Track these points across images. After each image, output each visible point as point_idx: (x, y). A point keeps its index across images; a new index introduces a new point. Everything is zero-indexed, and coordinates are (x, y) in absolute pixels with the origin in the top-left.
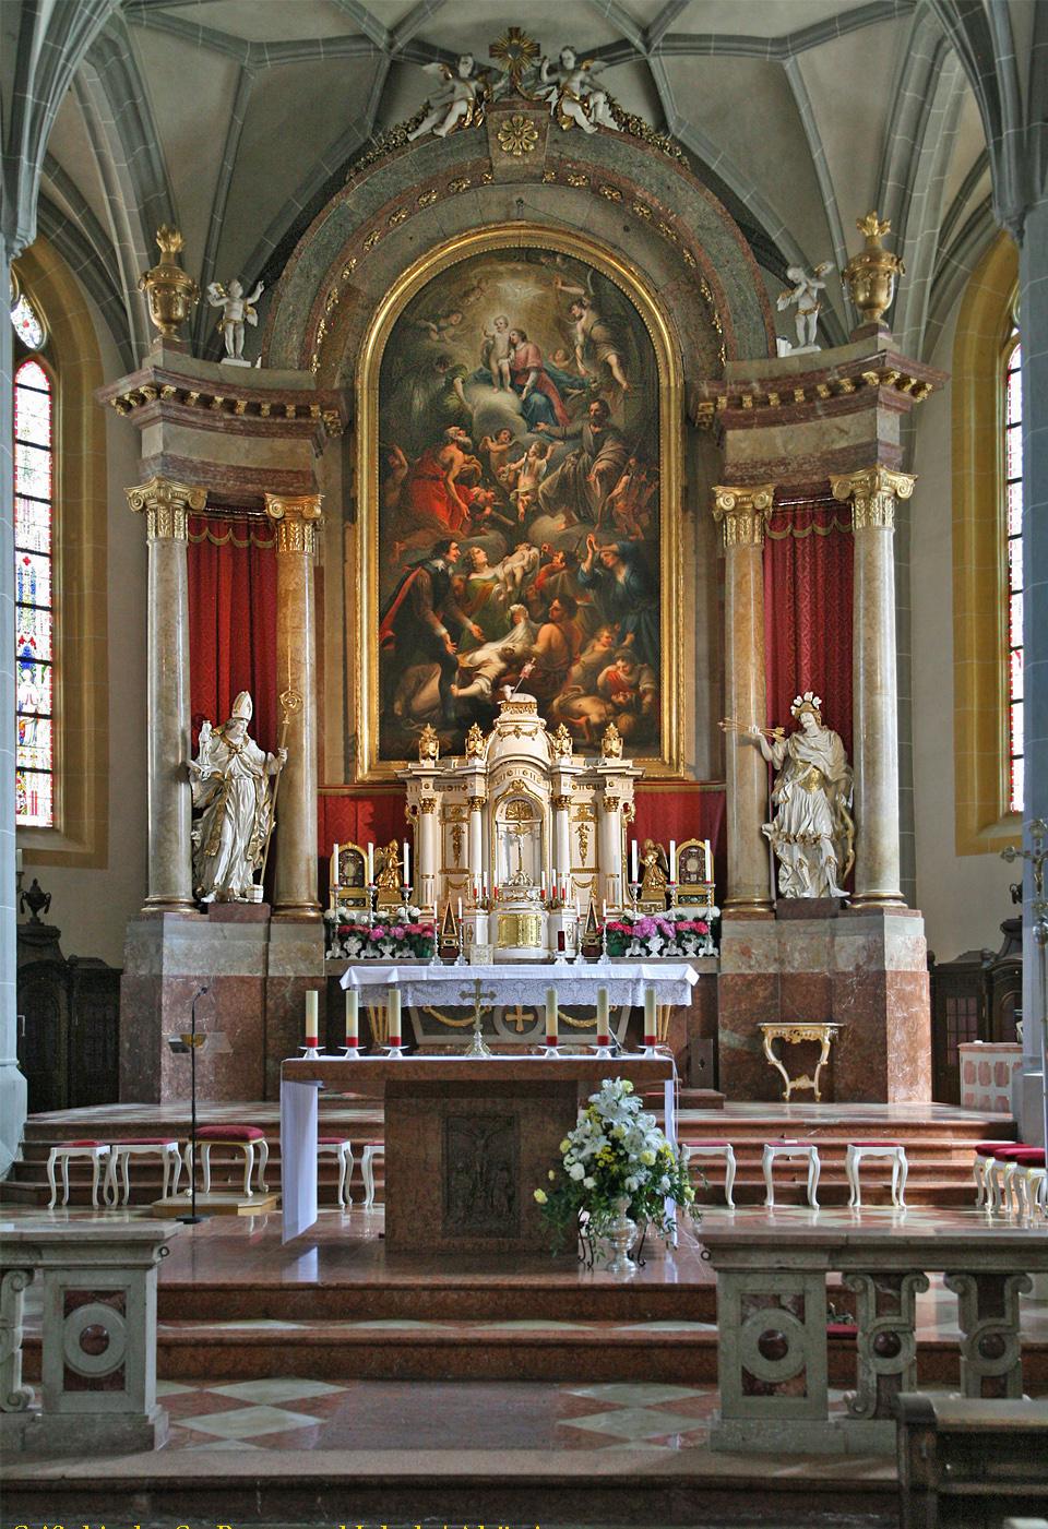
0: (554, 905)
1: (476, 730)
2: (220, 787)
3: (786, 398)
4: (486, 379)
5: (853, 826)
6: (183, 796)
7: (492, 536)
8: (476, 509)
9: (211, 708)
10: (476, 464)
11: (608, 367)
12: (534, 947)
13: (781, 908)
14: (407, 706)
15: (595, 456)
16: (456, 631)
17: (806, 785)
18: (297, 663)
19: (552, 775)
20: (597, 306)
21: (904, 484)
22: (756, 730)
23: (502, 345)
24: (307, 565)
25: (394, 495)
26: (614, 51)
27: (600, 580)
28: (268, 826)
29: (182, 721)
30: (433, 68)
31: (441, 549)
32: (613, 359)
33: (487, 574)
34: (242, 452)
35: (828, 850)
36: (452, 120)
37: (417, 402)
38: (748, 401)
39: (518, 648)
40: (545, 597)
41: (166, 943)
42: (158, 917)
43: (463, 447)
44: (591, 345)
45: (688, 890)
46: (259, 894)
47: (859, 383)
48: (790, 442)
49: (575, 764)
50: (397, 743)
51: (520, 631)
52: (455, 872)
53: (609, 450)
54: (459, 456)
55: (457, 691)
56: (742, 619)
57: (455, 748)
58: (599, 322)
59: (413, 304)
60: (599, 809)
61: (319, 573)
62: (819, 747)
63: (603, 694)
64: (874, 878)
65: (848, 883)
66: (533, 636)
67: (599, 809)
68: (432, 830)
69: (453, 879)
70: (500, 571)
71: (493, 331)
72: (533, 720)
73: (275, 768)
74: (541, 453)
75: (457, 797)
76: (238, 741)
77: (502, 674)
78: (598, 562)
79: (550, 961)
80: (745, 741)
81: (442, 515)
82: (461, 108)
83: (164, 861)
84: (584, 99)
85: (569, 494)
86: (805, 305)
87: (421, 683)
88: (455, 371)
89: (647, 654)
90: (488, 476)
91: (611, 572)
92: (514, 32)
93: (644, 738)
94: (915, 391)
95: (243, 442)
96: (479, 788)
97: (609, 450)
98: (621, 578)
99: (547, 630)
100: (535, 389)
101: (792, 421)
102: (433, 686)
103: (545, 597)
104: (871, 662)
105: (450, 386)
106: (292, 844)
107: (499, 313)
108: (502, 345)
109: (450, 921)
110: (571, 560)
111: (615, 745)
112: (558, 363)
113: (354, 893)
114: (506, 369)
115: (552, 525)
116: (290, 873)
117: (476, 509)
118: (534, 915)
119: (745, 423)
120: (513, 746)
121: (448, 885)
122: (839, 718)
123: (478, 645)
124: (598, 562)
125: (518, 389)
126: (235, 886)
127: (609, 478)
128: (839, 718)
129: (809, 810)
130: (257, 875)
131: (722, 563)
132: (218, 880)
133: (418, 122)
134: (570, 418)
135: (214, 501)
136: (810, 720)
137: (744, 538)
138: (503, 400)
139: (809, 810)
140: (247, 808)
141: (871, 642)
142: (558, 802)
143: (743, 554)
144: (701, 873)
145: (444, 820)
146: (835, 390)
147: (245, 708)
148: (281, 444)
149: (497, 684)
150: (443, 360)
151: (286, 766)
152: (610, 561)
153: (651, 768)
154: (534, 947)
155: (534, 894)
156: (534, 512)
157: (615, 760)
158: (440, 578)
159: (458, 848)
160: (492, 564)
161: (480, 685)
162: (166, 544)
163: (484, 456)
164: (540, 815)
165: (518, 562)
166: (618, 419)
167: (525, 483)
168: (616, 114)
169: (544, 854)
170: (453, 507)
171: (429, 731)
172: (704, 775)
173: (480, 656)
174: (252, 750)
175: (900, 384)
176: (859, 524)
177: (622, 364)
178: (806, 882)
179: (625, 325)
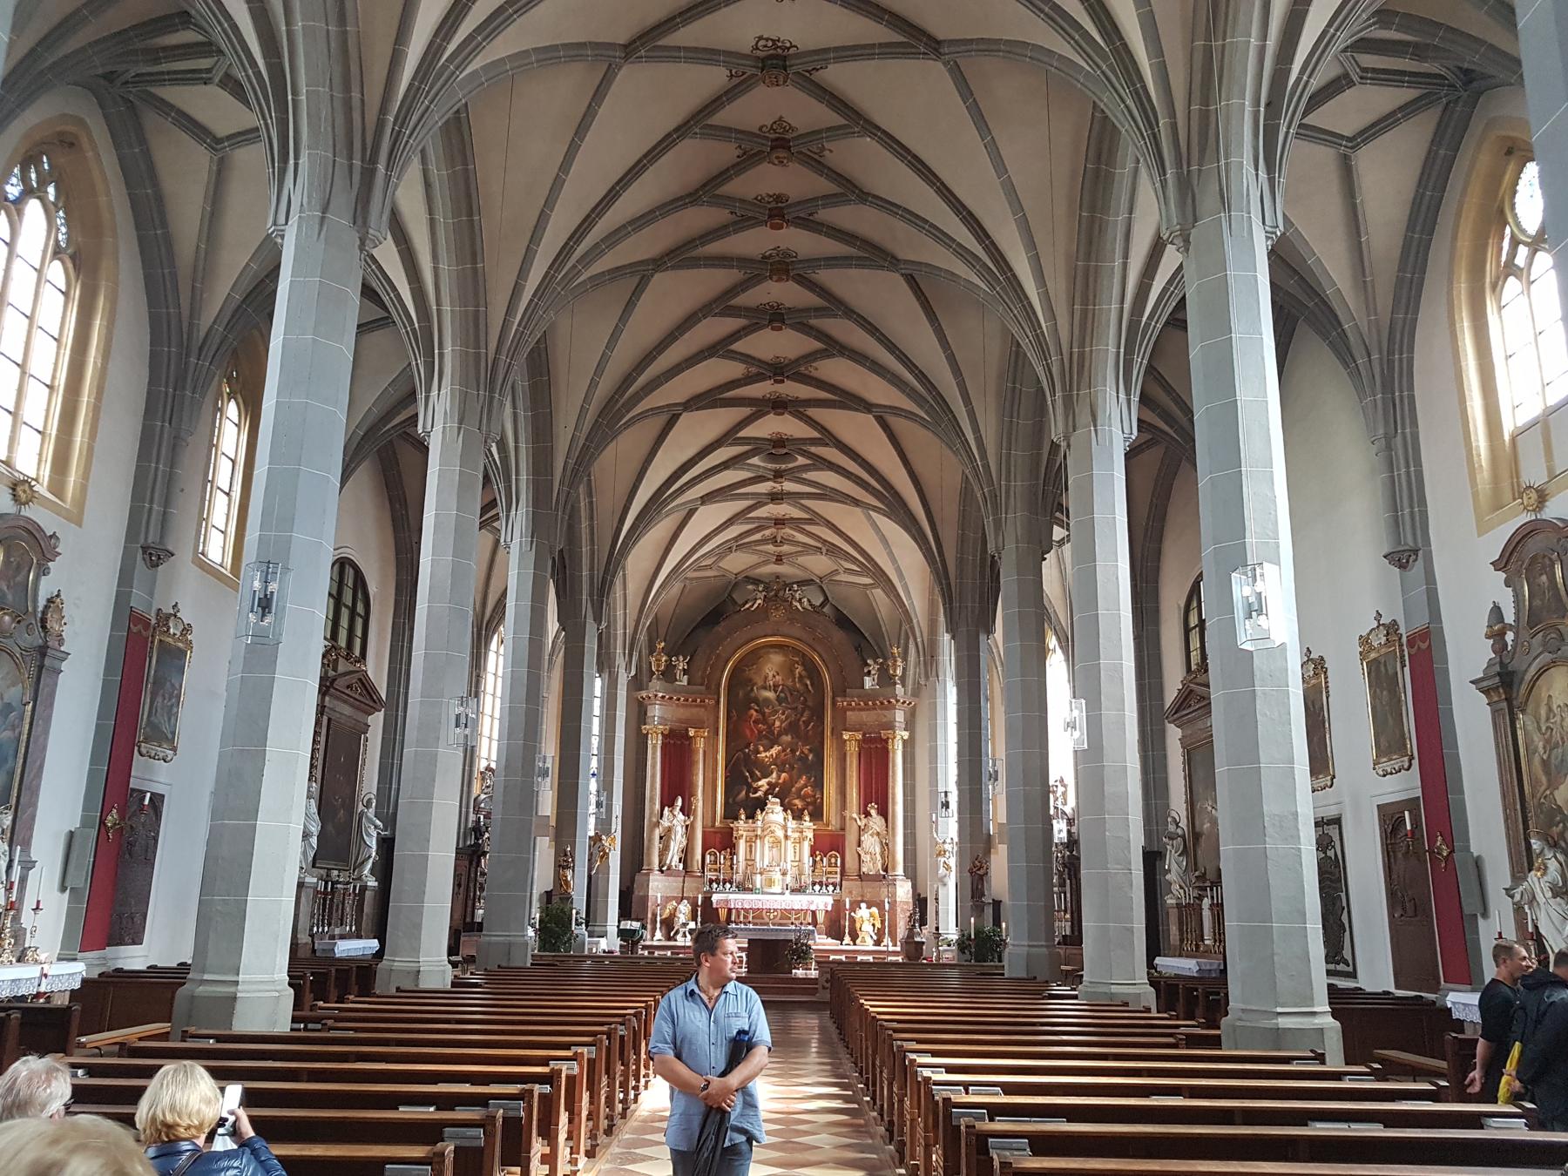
0: (784, 874)
1: (759, 812)
2: (669, 830)
3: (866, 704)
4: (765, 688)
5: (886, 848)
6: (657, 833)
7: (765, 742)
8: (760, 732)
9: (668, 802)
10: (760, 717)
11: (807, 685)
12: (777, 888)
13: (861, 877)
14: (734, 800)
15: (802, 716)
16: (752, 774)
17: (872, 835)
18: (697, 786)
19: (785, 828)
20: (803, 665)
21: (906, 735)
22: (855, 816)
23: (771, 674)
24: (701, 751)
25: (731, 727)
26: (809, 582)
27: (803, 758)
28: (685, 844)
29: (658, 806)
30: (750, 587)
31: (748, 746)
32: (808, 682)
33: (763, 755)
34: (683, 713)
35: (879, 857)
36: (756, 605)
37: (741, 694)
38: (853, 704)
39: (774, 781)
40: (784, 764)
41: (651, 884)
42: (648, 875)
43: (756, 711)
44: (801, 676)
45: (829, 869)
46: (681, 866)
47: (889, 702)
48: (867, 717)
49: (792, 824)
50: (731, 814)
51: (774, 775)
52: (750, 861)
53: (806, 714)
54: (755, 713)
55: (751, 795)
56: (851, 776)
57: (751, 816)
58: (805, 670)
59: (741, 660)
60: (800, 841)
61: (704, 752)
62: (876, 822)
63: (803, 798)
64: (894, 869)
65: (886, 870)
66: (779, 777)
67: (800, 841)
68: (742, 846)
69: (750, 863)
70: (768, 754)
71: (767, 671)
72: (779, 809)
73: (688, 823)
74: (783, 714)
75: (752, 834)
76: (676, 813)
77: (768, 790)
78: (802, 752)
79: (783, 894)
80: (852, 818)
81: (748, 732)
82: (759, 601)
83: (649, 855)
84: (800, 599)
85: (792, 728)
86: (873, 672)
87: (739, 793)
88: (755, 684)
89: (819, 785)
90: (765, 721)
91: (807, 756)
92: (778, 577)
93: (817, 815)
94: (910, 703)
95: (682, 710)
96: (759, 833)
97: (806, 714)
98: (810, 758)
99: (784, 774)
100: (781, 692)
101: (868, 710)
102: (744, 793)
103: (784, 764)
104: (894, 794)
105: (752, 690)
106: (693, 849)
107: (769, 665)
108: (771, 674)
109: (748, 877)
110: (793, 751)
111: (807, 818)
112: (789, 683)
113: (714, 867)
114: (771, 683)
115: (787, 738)
116: (692, 861)
117: (760, 732)
118: (777, 876)
119: (853, 709)
120: (772, 817)
121: (747, 865)
122: (884, 812)
123: (760, 780)
124: (802, 752)
125: (776, 692)
126: (673, 864)
127: (807, 723)
128: (884, 812)
129: (871, 843)
130: (680, 859)
131: (845, 754)
132: (668, 862)
133: (746, 602)
134: (794, 702)
135: (671, 730)
136: (873, 812)
137: (852, 749)
138: (770, 695)
139: (871, 843)
140: (679, 836)
141: (894, 788)
142: (786, 837)
143: (852, 754)
144: (836, 864)
145: (746, 841)
146: (882, 703)
147: (679, 802)
148: (695, 710)
149: (766, 794)
150: (750, 680)
151: (692, 823)
152: (806, 752)
153: (820, 826)
154: (777, 888)
155: (777, 869)
156: (780, 734)
157: (807, 823)
158: (747, 756)
159: (751, 852)
160: (765, 751)
161: (760, 793)
162: (654, 746)
163: (763, 714)
164: (780, 842)
165: (775, 750)
166: (810, 703)
167: (777, 724)
168: (811, 605)
169: (782, 858)
170: (752, 730)
171: (742, 811)
172: (838, 826)
173: (760, 783)
174: (681, 817)
175: (904, 702)
176: (890, 747)
177: (812, 685)
178: (871, 866)
179: (812, 672)
